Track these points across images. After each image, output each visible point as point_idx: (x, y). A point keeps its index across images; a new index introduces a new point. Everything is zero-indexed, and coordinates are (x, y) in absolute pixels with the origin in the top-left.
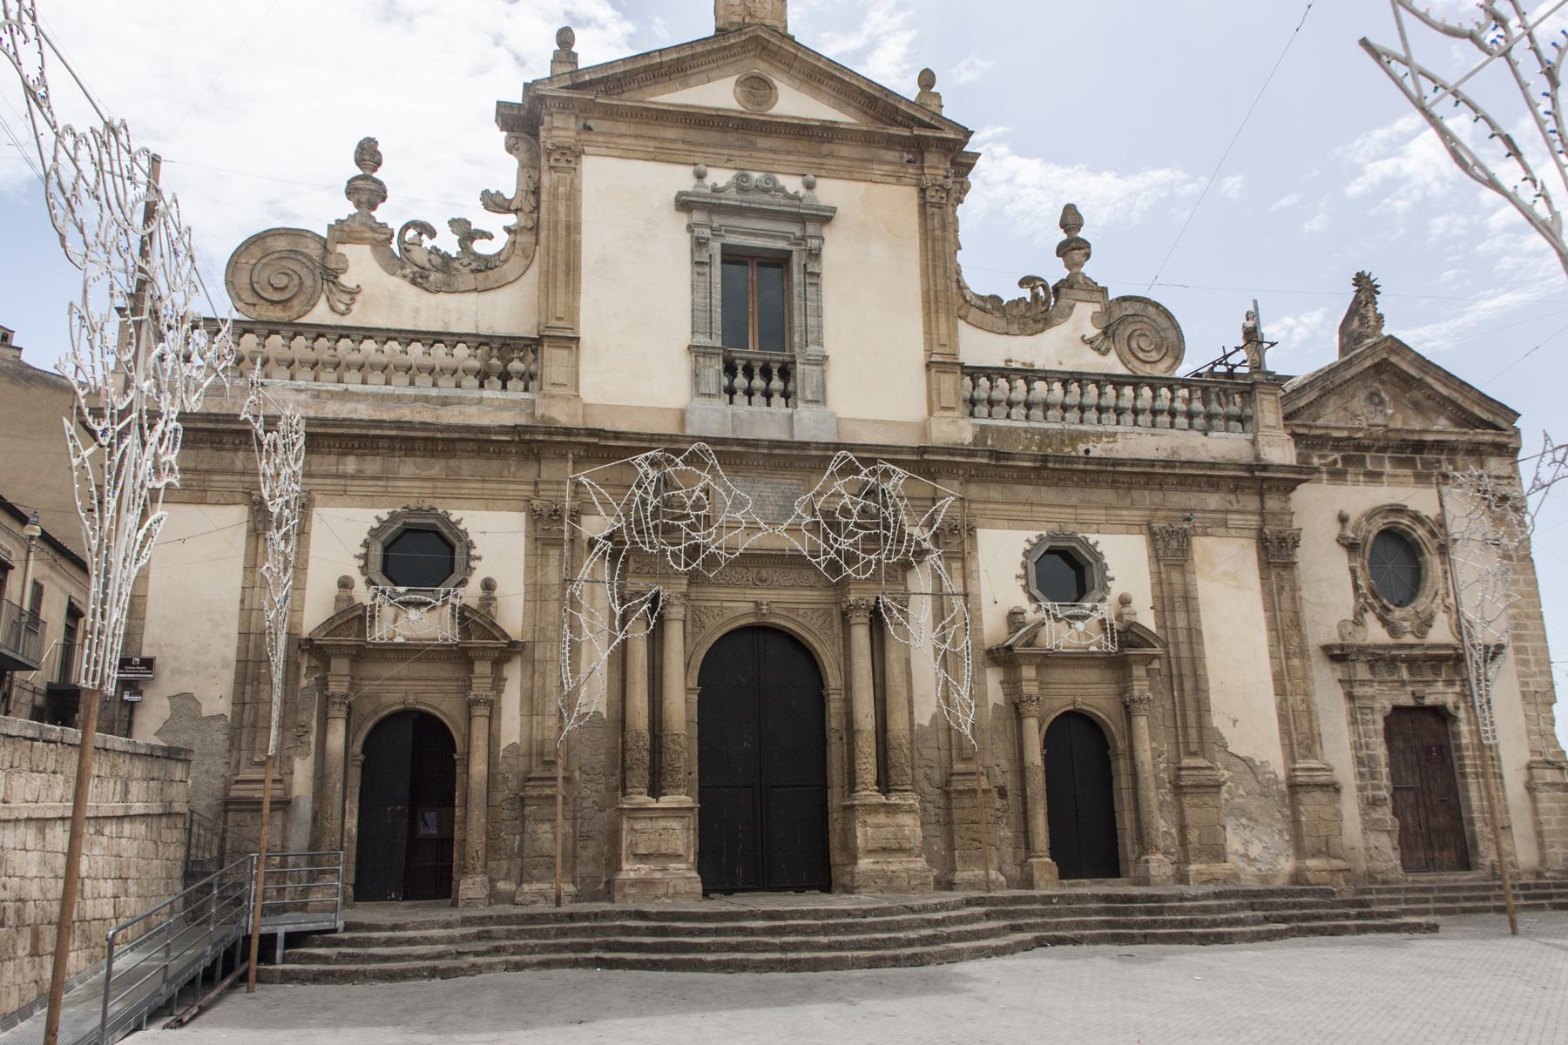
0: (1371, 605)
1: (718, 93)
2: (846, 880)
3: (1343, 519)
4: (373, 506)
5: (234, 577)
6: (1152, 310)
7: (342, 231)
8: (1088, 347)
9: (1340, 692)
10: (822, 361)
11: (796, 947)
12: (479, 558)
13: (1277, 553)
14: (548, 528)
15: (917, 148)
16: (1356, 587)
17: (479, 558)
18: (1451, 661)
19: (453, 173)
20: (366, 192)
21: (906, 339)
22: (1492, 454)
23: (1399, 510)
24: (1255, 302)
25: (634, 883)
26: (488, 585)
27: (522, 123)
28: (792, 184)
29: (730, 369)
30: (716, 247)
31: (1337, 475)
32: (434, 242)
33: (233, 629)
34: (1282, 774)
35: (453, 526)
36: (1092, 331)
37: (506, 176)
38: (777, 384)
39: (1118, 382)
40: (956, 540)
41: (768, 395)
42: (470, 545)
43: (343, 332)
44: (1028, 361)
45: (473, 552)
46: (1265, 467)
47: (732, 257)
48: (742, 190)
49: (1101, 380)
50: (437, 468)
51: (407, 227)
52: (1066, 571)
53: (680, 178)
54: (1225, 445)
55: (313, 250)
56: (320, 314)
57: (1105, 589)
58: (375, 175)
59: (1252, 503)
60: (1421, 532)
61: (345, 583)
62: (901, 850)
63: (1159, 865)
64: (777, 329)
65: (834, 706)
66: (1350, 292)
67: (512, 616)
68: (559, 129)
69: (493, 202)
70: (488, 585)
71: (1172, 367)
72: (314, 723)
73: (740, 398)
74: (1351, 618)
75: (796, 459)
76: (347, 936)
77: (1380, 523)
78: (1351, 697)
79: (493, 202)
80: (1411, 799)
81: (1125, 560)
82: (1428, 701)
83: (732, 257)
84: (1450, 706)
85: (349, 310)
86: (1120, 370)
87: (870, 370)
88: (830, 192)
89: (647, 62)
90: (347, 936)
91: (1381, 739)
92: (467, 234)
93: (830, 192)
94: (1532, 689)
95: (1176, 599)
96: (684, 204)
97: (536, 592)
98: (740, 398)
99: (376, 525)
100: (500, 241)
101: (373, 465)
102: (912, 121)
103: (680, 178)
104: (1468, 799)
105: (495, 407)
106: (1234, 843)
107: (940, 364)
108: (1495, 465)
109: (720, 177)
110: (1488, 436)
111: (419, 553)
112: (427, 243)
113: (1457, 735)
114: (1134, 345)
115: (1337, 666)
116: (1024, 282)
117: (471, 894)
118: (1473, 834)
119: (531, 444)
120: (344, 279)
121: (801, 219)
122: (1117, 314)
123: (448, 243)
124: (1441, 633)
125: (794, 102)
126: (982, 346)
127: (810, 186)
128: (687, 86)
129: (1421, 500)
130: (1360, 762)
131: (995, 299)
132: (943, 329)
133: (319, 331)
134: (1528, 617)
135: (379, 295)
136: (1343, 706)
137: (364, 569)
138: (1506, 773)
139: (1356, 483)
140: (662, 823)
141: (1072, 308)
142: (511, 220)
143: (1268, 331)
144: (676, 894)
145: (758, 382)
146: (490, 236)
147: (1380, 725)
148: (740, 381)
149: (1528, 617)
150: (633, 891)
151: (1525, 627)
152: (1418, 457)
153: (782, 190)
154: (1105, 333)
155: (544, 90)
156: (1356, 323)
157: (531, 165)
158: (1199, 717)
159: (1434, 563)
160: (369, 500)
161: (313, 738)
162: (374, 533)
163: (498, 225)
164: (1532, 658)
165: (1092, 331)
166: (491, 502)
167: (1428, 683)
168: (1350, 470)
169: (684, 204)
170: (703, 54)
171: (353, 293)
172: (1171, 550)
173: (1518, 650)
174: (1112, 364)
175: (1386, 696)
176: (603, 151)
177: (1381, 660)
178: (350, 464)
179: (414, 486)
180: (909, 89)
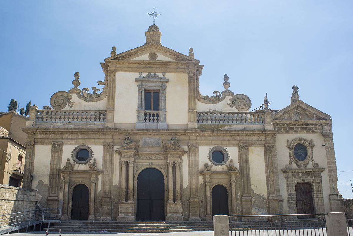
1: (145, 57)
3: (288, 141)
4: (74, 145)
5: (50, 159)
6: (244, 97)
7: (71, 91)
8: (228, 106)
9: (285, 180)
12: (94, 155)
13: (269, 150)
14: (108, 148)
16: (290, 156)
17: (94, 155)
19: (93, 78)
20: (76, 83)
21: (185, 105)
22: (325, 126)
23: (301, 139)
24: (267, 94)
25: (121, 218)
26: (95, 160)
27: (105, 66)
29: (146, 115)
30: (143, 89)
31: (287, 132)
32: (88, 92)
33: (49, 168)
34: (266, 198)
36: (229, 102)
37: (102, 77)
39: (237, 113)
40: (193, 149)
41: (150, 120)
42: (92, 152)
44: (214, 110)
45: (93, 153)
49: (233, 113)
51: (83, 89)
52: (218, 156)
53: (136, 75)
55: (66, 95)
57: (228, 159)
58: (78, 80)
59: (263, 138)
60: (306, 144)
61: (68, 160)
62: (177, 213)
66: (291, 91)
67: (100, 165)
68: (112, 67)
69: (100, 83)
71: (248, 110)
72: (63, 186)
73: (148, 121)
74: (289, 163)
77: (296, 142)
78: (287, 181)
79: (100, 83)
80: (301, 203)
81: (233, 153)
82: (306, 182)
84: (311, 182)
85: (72, 106)
86: (236, 111)
89: (129, 52)
91: (294, 190)
92: (95, 89)
93: (168, 76)
94: (332, 178)
95: (244, 161)
96: (136, 81)
97: (105, 161)
98: (148, 121)
99: (75, 148)
100: (102, 90)
101: (74, 137)
103: (136, 75)
104: (314, 203)
105: (98, 124)
106: (254, 211)
107: (191, 110)
108: (326, 128)
110: (324, 121)
111: (83, 155)
112: (87, 92)
113: (313, 188)
114: (239, 105)
115: (284, 174)
116: (214, 92)
117: (91, 219)
119: (103, 131)
120: (71, 100)
122: (236, 98)
123: (91, 92)
125: (161, 57)
126: (202, 107)
128: (138, 56)
130: (289, 195)
131: (207, 97)
132: (192, 104)
134: (332, 162)
135: (78, 103)
136: (285, 183)
138: (324, 197)
139: (292, 133)
140: (127, 206)
141: (225, 97)
142: (103, 86)
143: (269, 100)
144: (129, 220)
145: (152, 118)
146: (99, 90)
147: (294, 187)
148: (148, 118)
149: (332, 162)
150: (121, 219)
152: (307, 127)
153: (158, 76)
154: (232, 102)
155: (108, 60)
156: (293, 97)
158: (247, 186)
160: (73, 144)
161: (63, 189)
163: (100, 87)
164: (332, 171)
165: (229, 102)
166: (96, 144)
167: (306, 177)
168: (290, 130)
170: (141, 49)
172: (244, 149)
173: (329, 170)
175: (296, 180)
176: (120, 71)
178: (70, 137)
180: (186, 53)
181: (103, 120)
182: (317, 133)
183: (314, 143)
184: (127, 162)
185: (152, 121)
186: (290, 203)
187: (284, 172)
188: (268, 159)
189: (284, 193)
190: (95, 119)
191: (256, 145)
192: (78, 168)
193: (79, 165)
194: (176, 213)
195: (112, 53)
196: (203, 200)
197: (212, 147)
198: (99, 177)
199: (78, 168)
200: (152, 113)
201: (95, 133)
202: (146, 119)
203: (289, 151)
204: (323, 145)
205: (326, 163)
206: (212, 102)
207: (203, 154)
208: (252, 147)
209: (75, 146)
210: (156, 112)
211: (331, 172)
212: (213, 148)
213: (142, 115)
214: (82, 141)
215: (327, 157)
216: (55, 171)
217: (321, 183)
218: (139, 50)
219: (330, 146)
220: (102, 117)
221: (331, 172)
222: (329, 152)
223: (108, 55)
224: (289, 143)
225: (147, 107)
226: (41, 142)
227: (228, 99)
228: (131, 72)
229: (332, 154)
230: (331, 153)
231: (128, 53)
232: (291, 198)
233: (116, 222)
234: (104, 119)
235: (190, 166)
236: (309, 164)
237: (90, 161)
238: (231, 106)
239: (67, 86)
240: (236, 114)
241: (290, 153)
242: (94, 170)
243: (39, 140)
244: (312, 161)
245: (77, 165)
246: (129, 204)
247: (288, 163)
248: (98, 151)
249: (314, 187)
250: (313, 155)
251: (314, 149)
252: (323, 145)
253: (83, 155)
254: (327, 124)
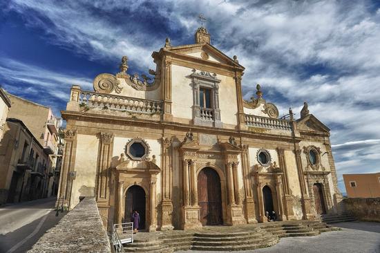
2: (229, 222)
10: (219, 111)
11: (242, 243)
13: (297, 152)
15: (235, 70)
23: (313, 146)
26: (154, 157)
30: (198, 86)
35: (145, 143)
38: (211, 115)
40: (243, 150)
43: (122, 97)
47: (202, 88)
48: (202, 74)
49: (264, 118)
50: (142, 129)
52: (264, 157)
53: (189, 71)
54: (288, 133)
56: (113, 93)
63: (284, 217)
64: (209, 105)
65: (223, 184)
67: (158, 163)
70: (154, 157)
75: (213, 131)
76: (135, 244)
87: (227, 116)
88: (219, 77)
90: (135, 244)
93: (219, 77)
95: (282, 161)
101: (128, 128)
102: (234, 65)
103: (189, 71)
107: (239, 114)
109: (198, 72)
111: (138, 149)
120: (119, 86)
121: (214, 82)
124: (320, 170)
125: (211, 59)
129: (318, 145)
133: (116, 97)
137: (126, 152)
145: (207, 115)
157: (159, 66)
160: (126, 136)
162: (128, 144)
166: (153, 137)
169: (191, 77)
171: (121, 89)
172: (280, 151)
174: (267, 116)
177: (312, 174)
179: (138, 133)
207: (253, 153)
210: (211, 110)
220: (158, 107)
245: (131, 162)
248: (155, 148)
253: (138, 149)
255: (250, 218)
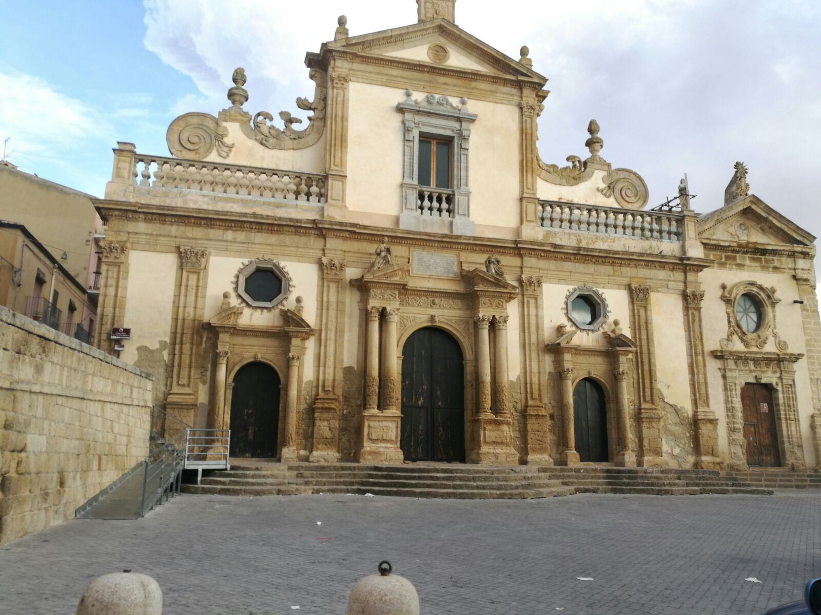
0: (736, 332)
1: (419, 53)
2: (474, 457)
3: (724, 287)
4: (241, 257)
5: (170, 290)
6: (632, 176)
7: (225, 115)
8: (599, 194)
9: (719, 374)
10: (468, 195)
11: (460, 487)
12: (294, 286)
13: (691, 301)
14: (328, 271)
15: (519, 85)
16: (729, 322)
17: (294, 286)
18: (781, 361)
20: (236, 95)
21: (510, 183)
22: (800, 258)
23: (753, 284)
24: (686, 175)
25: (370, 453)
26: (299, 300)
27: (319, 63)
28: (455, 101)
29: (421, 197)
30: (415, 133)
31: (722, 265)
32: (273, 123)
33: (168, 316)
34: (690, 414)
35: (281, 270)
36: (602, 186)
37: (309, 89)
38: (444, 205)
39: (616, 212)
42: (290, 279)
43: (227, 167)
44: (570, 199)
45: (291, 283)
46: (689, 259)
47: (425, 138)
48: (429, 102)
50: (273, 239)
51: (259, 115)
53: (396, 96)
54: (669, 247)
55: (211, 125)
56: (213, 157)
57: (605, 316)
58: (243, 87)
59: (679, 276)
60: (763, 295)
61: (226, 296)
62: (502, 443)
63: (630, 458)
64: (446, 178)
65: (469, 368)
66: (733, 171)
67: (310, 316)
68: (339, 67)
69: (303, 104)
70: (299, 300)
71: (642, 206)
72: (209, 366)
73: (426, 211)
74: (726, 337)
76: (232, 472)
77: (742, 290)
78: (724, 377)
79: (303, 104)
80: (752, 429)
81: (617, 304)
82: (763, 381)
83: (425, 138)
84: (774, 384)
85: (228, 156)
86: (616, 206)
87: (490, 202)
88: (473, 106)
89: (385, 35)
90: (232, 472)
91: (739, 399)
92: (289, 120)
93: (473, 106)
94: (816, 377)
95: (641, 324)
96: (400, 110)
97: (322, 306)
98: (426, 211)
99: (242, 267)
100: (306, 124)
101: (241, 236)
102: (517, 72)
103: (396, 96)
104: (781, 431)
105: (304, 210)
106: (665, 448)
108: (801, 263)
109: (418, 96)
110: (798, 248)
111: (265, 283)
112: (269, 123)
113: (777, 398)
114: (623, 193)
115: (718, 361)
116: (568, 159)
117: (288, 456)
118: (783, 449)
119: (320, 230)
120: (226, 140)
121: (459, 120)
122: (615, 177)
123: (279, 124)
124: (770, 348)
125: (457, 60)
126: (547, 190)
127: (463, 103)
128: (403, 48)
129: (766, 279)
130: (728, 410)
131: (554, 166)
132: (530, 180)
133: (215, 166)
134: (815, 341)
135: (242, 148)
136: (720, 381)
137: (236, 289)
138: (801, 418)
139: (731, 269)
140: (385, 424)
141: (593, 173)
142: (311, 113)
143: (691, 191)
144: (391, 459)
145: (435, 204)
146: (300, 122)
147: (739, 392)
148: (426, 203)
149: (815, 341)
150: (369, 457)
151: (814, 346)
152: (763, 257)
153: (451, 105)
154: (609, 187)
155: (332, 47)
156: (735, 188)
157: (322, 87)
158: (651, 383)
159: (769, 310)
160: (239, 254)
161: (208, 374)
162: (241, 271)
163: (304, 115)
164: (816, 361)
165: (602, 186)
166: (300, 258)
167: (763, 372)
168: (728, 262)
169: (400, 110)
170: (412, 32)
171: (230, 147)
172: (638, 296)
173: (809, 357)
174: (611, 202)
175: (742, 377)
176: (360, 80)
177: (739, 358)
178: (230, 235)
180: (516, 57)
181: (317, 199)
182: (784, 273)
183: (777, 295)
184: (384, 309)
185: (435, 212)
186: (732, 430)
187: (716, 357)
188: (693, 323)
189: (717, 407)
190: (297, 193)
191: (666, 290)
192: (251, 319)
193: (254, 312)
194: (499, 443)
195: (338, 32)
196: (556, 414)
197: (573, 287)
198: (306, 346)
199: (251, 319)
200: (437, 194)
201: (299, 230)
202: (422, 208)
203: (727, 308)
204: (795, 302)
205: (803, 344)
206: (564, 181)
207: (554, 301)
208: (658, 295)
209: (242, 260)
210: (445, 191)
211: (813, 364)
212: (575, 290)
213: (413, 197)
214: (586, 277)
215: (805, 329)
216: (188, 323)
217: (795, 387)
218: (408, 33)
219: (810, 305)
220: (314, 189)
221: (813, 364)
222: (808, 317)
223: (328, 35)
224: (727, 290)
225: (424, 179)
226: (147, 243)
227: (597, 179)
228: (386, 86)
229: (814, 323)
230: (813, 321)
231: (382, 35)
232: (733, 416)
233: (355, 465)
234: (320, 195)
235: (524, 328)
236: (768, 342)
237: (284, 302)
238: (605, 195)
239: (215, 101)
240: (621, 213)
241: (728, 314)
242: (291, 327)
243: (140, 236)
244: (775, 335)
245: (247, 311)
246: (388, 419)
247: (726, 337)
248: (303, 281)
249: (781, 395)
250: (776, 321)
251: (777, 306)
252: (795, 302)
253: (265, 283)
254: (805, 255)
255: (534, 451)
